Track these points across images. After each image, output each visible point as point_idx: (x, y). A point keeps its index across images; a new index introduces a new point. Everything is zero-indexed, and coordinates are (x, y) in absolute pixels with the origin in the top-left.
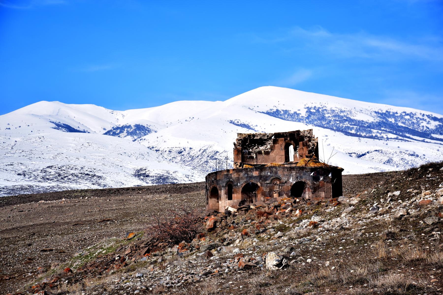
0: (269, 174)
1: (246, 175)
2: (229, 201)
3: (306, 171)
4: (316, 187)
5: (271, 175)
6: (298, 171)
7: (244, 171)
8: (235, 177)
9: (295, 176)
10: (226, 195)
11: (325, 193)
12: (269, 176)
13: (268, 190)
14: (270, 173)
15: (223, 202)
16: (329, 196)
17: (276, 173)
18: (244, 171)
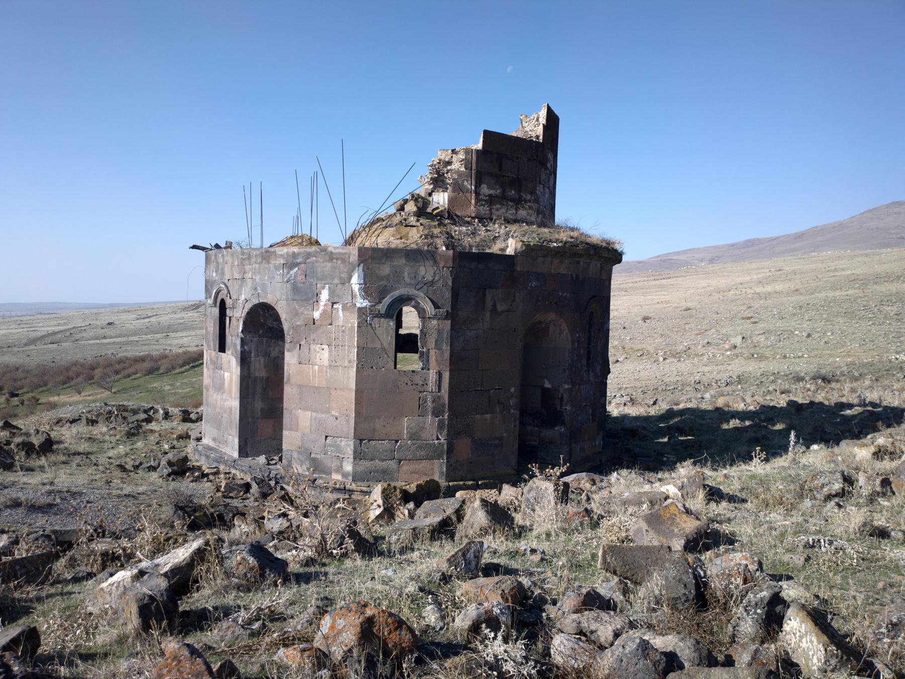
0: (214, 274)
3: (275, 267)
4: (300, 326)
6: (257, 266)
9: (249, 283)
11: (330, 352)
14: (216, 272)
16: (346, 364)
17: (223, 274)
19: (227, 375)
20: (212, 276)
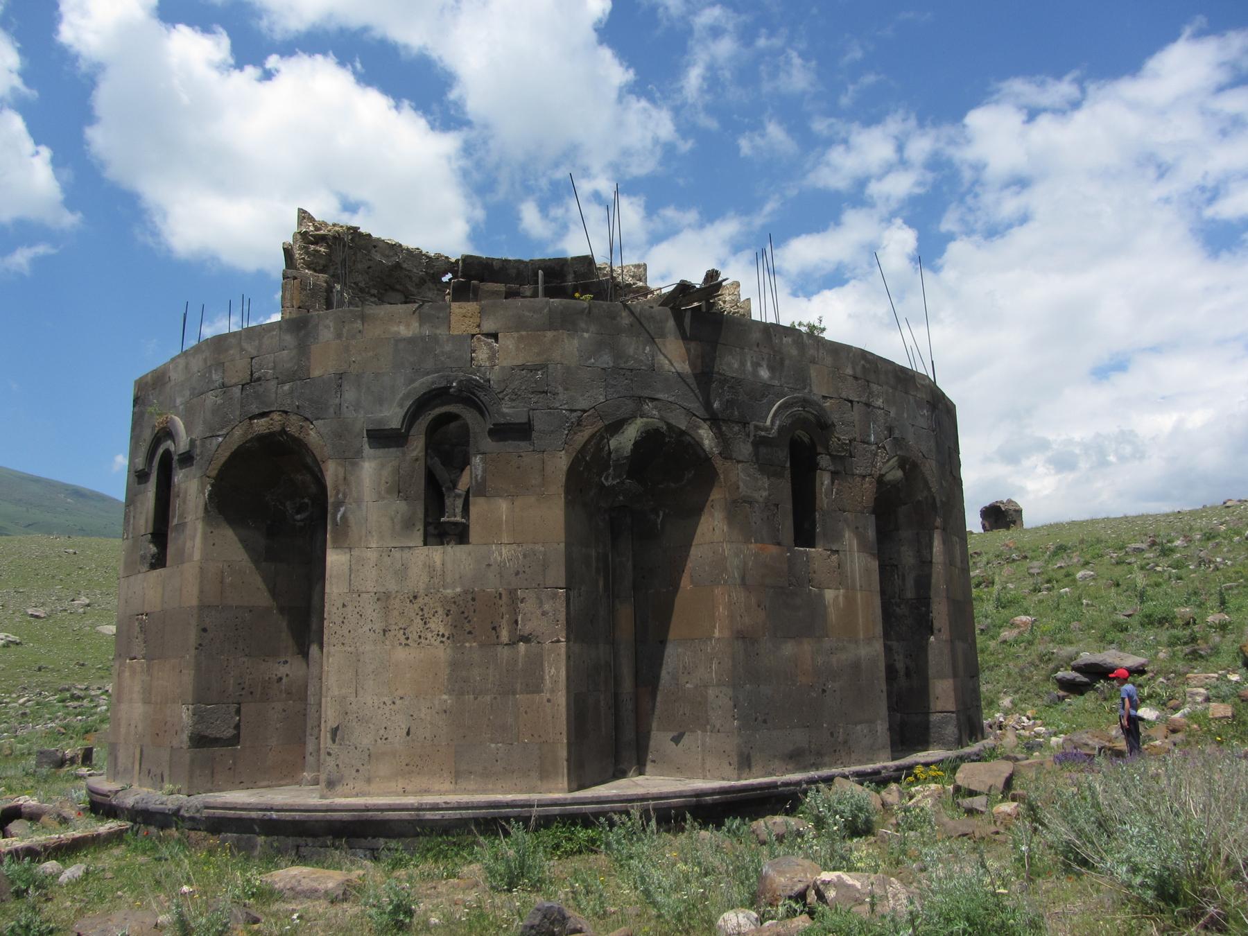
0: (764, 373)
1: (606, 360)
2: (436, 554)
5: (776, 383)
7: (593, 328)
8: (505, 362)
10: (401, 506)
12: (767, 387)
13: (765, 494)
14: (771, 369)
15: (372, 555)
17: (802, 379)
18: (593, 328)
19: (829, 594)
20: (755, 373)
